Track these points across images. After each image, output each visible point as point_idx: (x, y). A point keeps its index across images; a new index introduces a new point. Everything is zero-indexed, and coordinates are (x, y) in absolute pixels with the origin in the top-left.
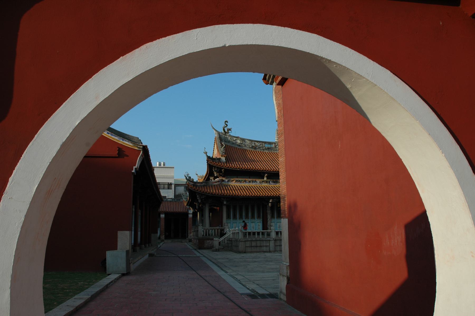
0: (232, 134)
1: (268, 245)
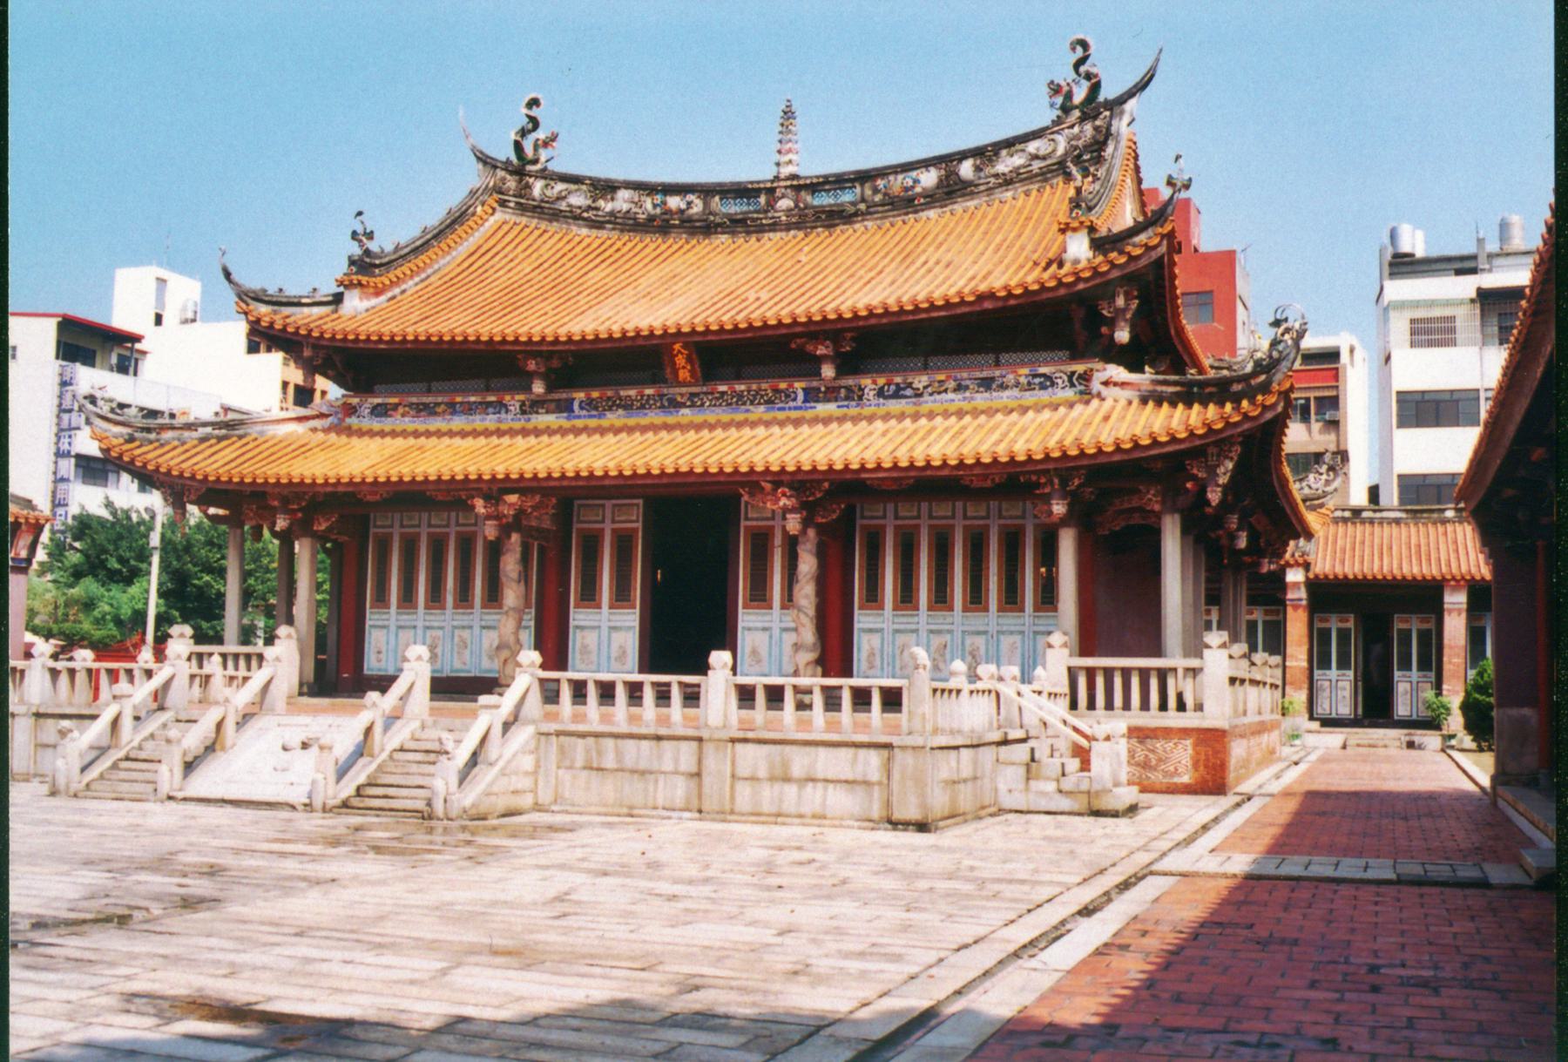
0: (556, 167)
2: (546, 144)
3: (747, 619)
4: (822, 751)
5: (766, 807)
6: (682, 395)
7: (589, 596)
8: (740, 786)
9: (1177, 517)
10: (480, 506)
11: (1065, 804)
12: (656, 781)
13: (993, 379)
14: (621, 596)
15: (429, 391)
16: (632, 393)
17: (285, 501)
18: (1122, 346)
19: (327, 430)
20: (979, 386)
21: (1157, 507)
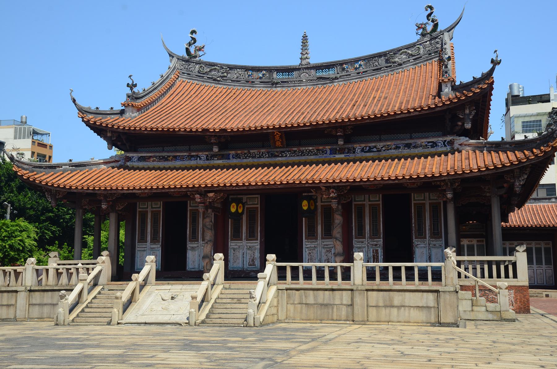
0: (204, 59)
1: (13, 302)
2: (200, 50)
3: (306, 244)
4: (407, 294)
5: (383, 319)
6: (277, 152)
7: (237, 236)
8: (370, 309)
9: (499, 198)
10: (198, 198)
11: (490, 316)
12: (333, 308)
13: (411, 144)
14: (251, 236)
15: (163, 151)
16: (256, 151)
17: (105, 196)
18: (468, 129)
19: (119, 168)
20: (405, 146)
21: (488, 195)
